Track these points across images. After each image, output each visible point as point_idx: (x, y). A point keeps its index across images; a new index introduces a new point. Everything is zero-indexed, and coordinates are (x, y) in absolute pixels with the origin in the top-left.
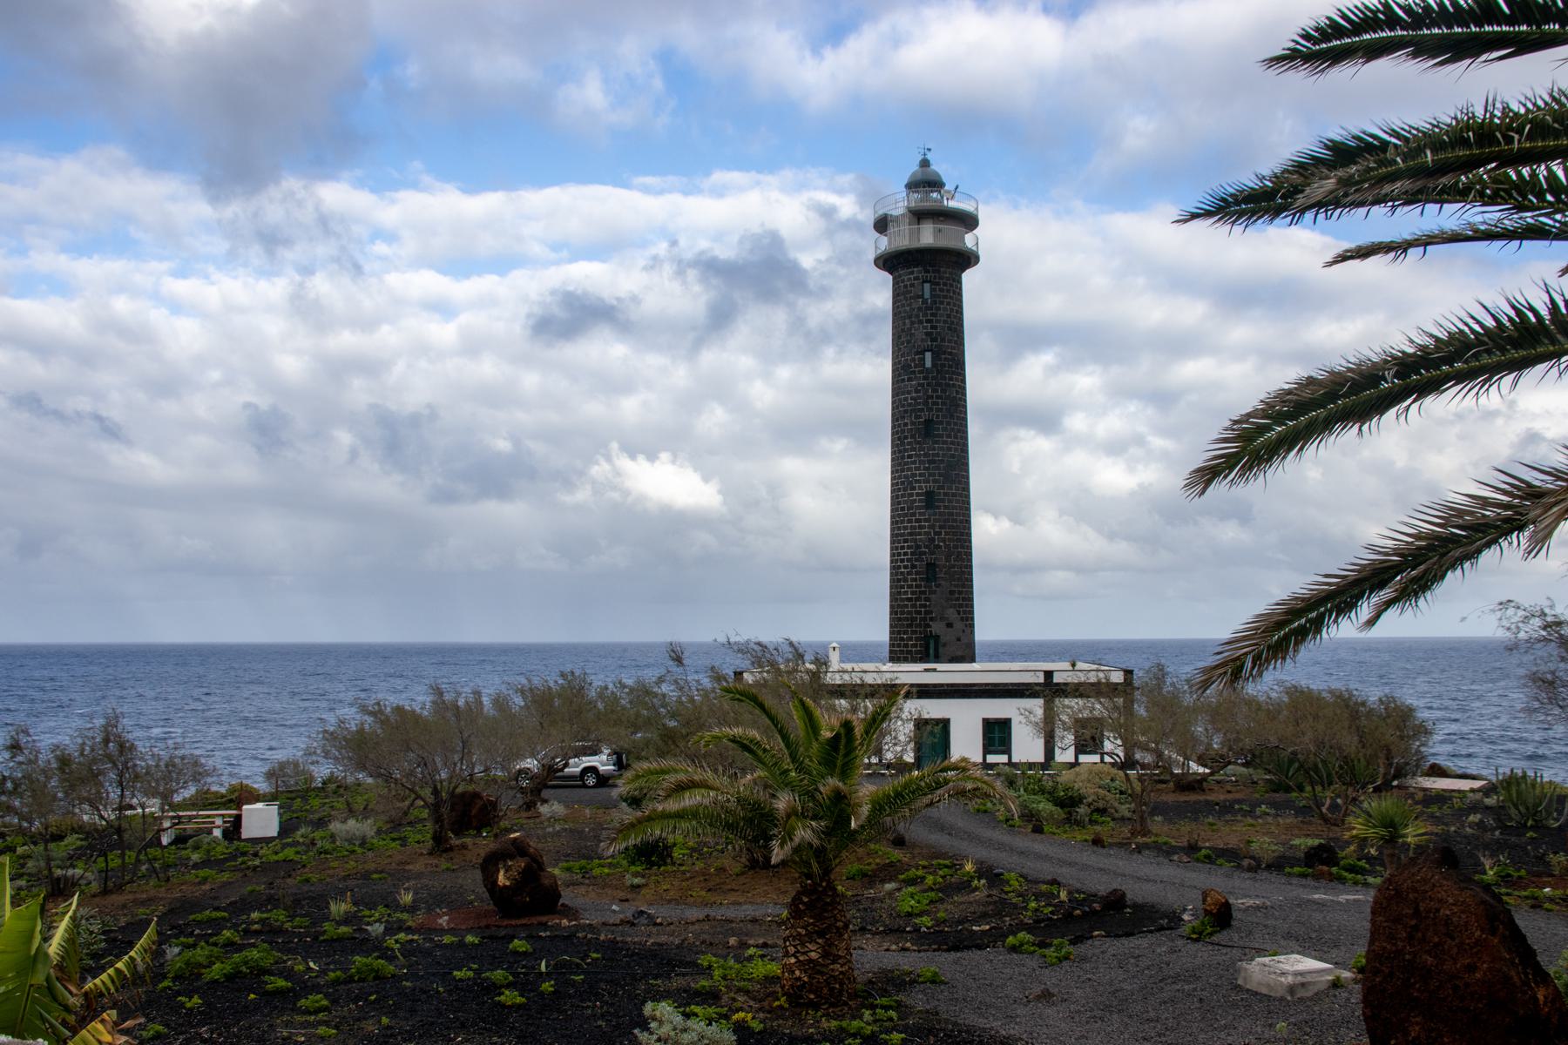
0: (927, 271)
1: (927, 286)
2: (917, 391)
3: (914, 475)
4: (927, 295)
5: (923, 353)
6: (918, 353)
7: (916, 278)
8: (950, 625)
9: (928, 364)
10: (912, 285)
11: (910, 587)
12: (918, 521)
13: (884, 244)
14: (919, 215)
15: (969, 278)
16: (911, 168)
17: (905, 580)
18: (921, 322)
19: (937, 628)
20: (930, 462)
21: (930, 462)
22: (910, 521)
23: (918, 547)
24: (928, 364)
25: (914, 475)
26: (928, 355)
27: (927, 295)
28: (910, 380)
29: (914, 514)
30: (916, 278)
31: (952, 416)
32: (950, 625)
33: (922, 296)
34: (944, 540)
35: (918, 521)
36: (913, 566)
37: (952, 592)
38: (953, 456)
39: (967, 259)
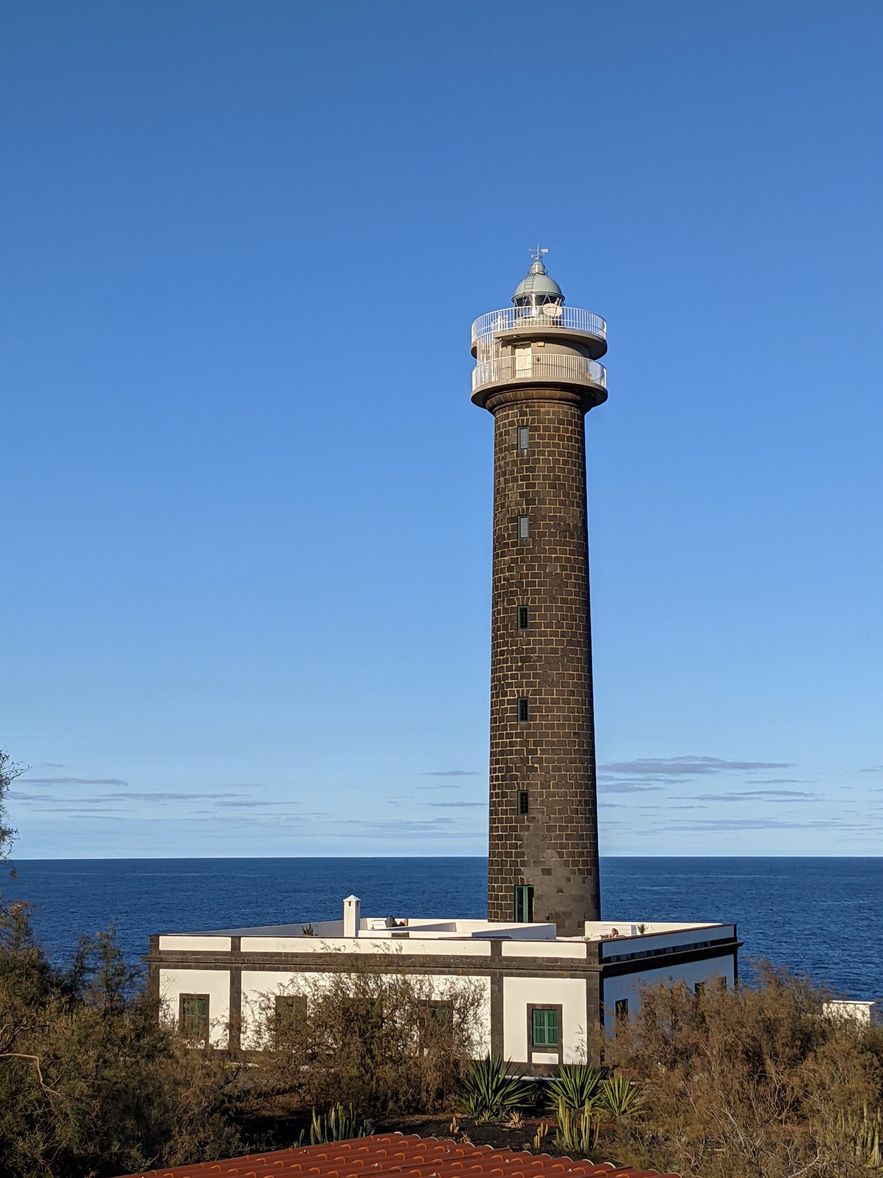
2: (510, 569)
3: (506, 677)
4: (524, 444)
6: (512, 520)
8: (547, 872)
9: (524, 533)
12: (509, 736)
18: (515, 480)
19: (530, 875)
20: (523, 660)
21: (523, 660)
23: (509, 769)
24: (524, 533)
26: (524, 522)
27: (524, 444)
30: (511, 424)
32: (547, 872)
33: (516, 447)
34: (540, 760)
35: (509, 736)
36: (504, 795)
37: (550, 828)
38: (554, 651)
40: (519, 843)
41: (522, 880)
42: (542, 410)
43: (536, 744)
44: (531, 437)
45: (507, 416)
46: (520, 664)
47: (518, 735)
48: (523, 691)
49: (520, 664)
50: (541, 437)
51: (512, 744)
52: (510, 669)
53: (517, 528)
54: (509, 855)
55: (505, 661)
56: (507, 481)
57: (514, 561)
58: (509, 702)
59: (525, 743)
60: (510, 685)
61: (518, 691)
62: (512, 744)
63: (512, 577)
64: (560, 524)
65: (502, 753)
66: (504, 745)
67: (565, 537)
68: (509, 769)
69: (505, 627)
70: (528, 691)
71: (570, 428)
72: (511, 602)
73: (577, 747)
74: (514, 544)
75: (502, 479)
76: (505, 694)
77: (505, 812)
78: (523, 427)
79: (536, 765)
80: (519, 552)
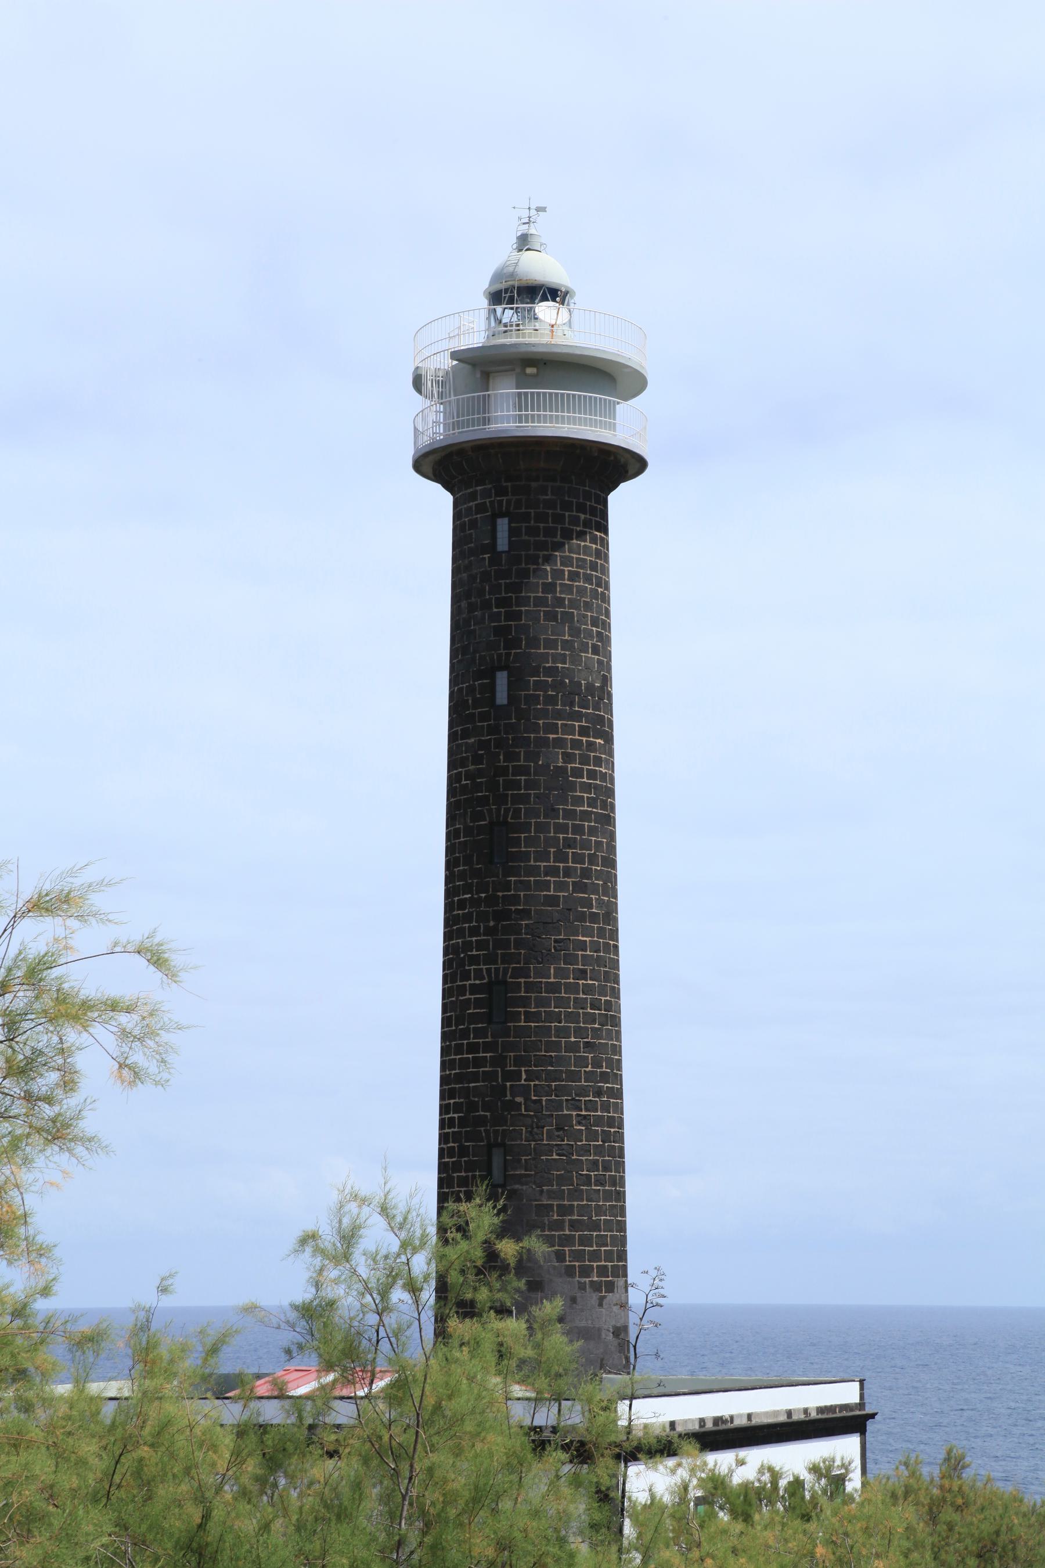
0: (501, 492)
1: (503, 525)
2: (477, 760)
3: (467, 946)
4: (502, 543)
5: (490, 673)
6: (479, 675)
9: (502, 697)
10: (473, 524)
12: (473, 1048)
16: (492, 257)
18: (486, 605)
23: (472, 1107)
25: (467, 946)
27: (502, 543)
29: (465, 1034)
31: (553, 812)
35: (473, 1048)
42: (534, 484)
43: (519, 1061)
44: (512, 532)
45: (473, 496)
46: (492, 923)
47: (487, 1047)
49: (492, 923)
50: (533, 531)
51: (478, 1062)
52: (474, 931)
53: (492, 688)
55: (468, 918)
56: (472, 608)
57: (483, 745)
58: (474, 989)
59: (499, 1061)
60: (474, 960)
61: (489, 970)
62: (478, 1062)
63: (480, 773)
64: (562, 683)
65: (459, 1078)
66: (464, 1063)
67: (572, 704)
68: (472, 1107)
69: (468, 860)
70: (506, 970)
71: (582, 516)
72: (477, 816)
73: (590, 1069)
74: (484, 717)
75: (464, 604)
76: (466, 976)
78: (502, 515)
79: (519, 1099)
80: (493, 730)
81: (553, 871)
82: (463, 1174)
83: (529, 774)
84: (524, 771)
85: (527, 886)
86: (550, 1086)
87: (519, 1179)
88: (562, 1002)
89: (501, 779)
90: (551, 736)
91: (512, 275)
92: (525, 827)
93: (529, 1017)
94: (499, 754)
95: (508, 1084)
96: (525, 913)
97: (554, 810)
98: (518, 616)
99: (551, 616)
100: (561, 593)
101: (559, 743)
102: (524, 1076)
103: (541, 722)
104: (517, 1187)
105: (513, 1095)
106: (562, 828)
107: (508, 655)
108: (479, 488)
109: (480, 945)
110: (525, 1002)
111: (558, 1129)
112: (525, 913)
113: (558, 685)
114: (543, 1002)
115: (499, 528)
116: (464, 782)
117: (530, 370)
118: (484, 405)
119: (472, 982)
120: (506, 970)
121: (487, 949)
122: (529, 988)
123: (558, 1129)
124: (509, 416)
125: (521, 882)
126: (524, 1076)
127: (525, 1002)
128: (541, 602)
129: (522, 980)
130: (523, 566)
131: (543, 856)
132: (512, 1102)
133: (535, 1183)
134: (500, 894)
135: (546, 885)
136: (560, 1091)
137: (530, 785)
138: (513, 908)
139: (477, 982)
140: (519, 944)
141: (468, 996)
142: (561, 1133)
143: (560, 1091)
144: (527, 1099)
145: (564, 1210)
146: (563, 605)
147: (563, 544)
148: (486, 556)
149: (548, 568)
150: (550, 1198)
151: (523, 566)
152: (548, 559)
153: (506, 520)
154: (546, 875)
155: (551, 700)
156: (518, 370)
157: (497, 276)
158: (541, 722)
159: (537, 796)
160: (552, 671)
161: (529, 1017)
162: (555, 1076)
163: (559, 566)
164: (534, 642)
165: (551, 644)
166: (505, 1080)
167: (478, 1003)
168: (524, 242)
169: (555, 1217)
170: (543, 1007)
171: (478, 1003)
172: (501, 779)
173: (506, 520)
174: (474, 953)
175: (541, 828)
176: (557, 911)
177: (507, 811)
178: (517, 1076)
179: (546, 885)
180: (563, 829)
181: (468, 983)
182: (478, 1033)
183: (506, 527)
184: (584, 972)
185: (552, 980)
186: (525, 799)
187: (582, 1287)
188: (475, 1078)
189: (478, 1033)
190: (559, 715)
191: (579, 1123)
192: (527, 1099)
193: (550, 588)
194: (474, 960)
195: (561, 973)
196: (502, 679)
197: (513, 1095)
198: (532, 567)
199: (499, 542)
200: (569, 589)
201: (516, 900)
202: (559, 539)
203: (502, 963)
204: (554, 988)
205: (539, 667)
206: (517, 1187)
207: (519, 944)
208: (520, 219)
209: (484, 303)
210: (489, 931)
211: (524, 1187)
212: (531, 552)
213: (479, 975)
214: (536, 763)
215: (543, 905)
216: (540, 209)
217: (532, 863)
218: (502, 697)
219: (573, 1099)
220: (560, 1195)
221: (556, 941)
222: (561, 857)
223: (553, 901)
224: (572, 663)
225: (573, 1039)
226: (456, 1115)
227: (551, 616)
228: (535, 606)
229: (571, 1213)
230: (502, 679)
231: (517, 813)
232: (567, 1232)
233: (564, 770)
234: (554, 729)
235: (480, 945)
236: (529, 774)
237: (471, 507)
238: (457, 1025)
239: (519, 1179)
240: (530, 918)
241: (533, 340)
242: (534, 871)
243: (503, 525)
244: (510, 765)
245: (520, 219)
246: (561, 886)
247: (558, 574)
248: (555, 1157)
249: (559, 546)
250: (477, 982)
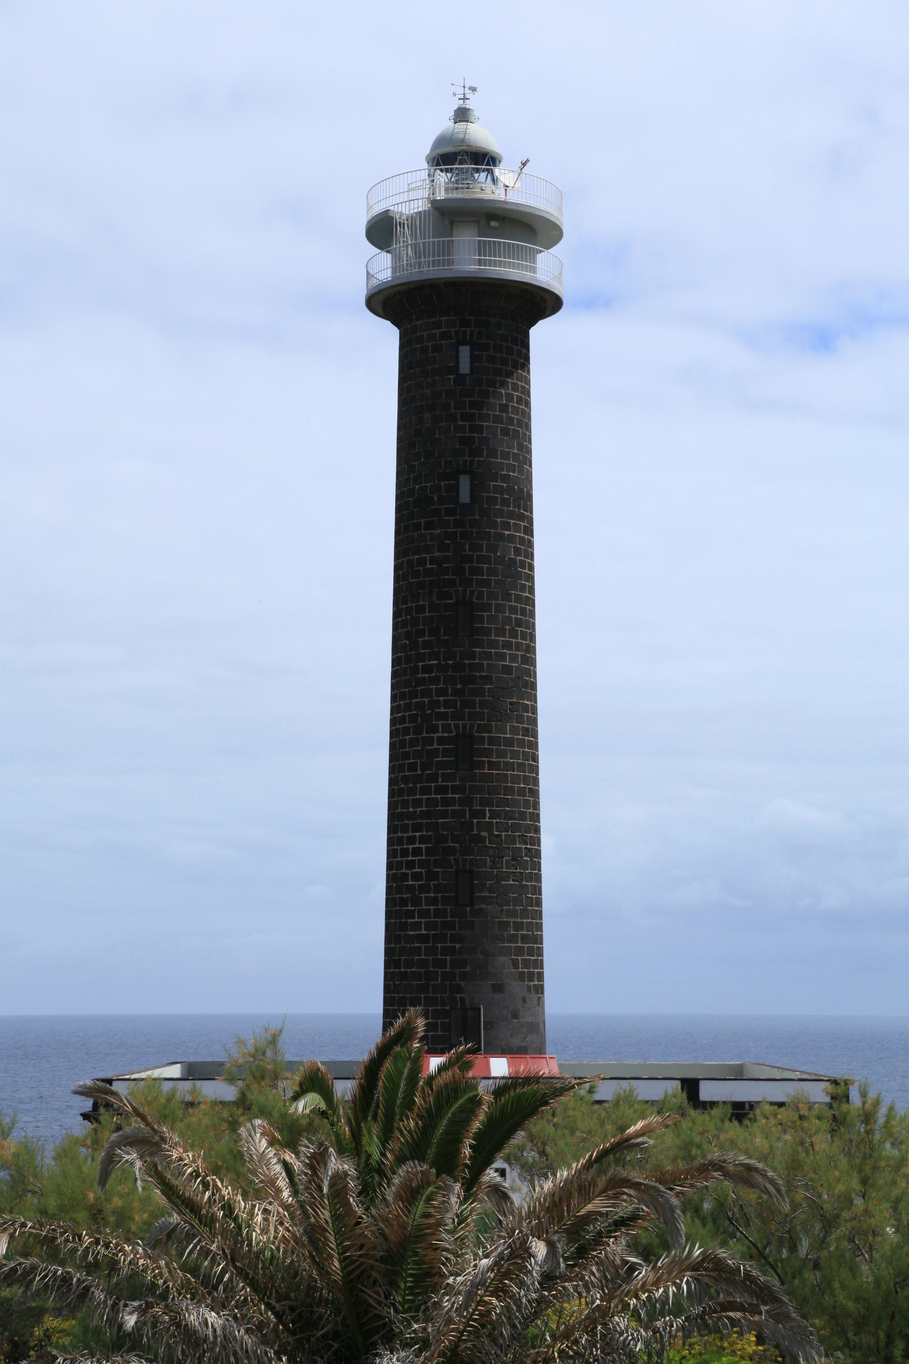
1: (465, 352)
3: (434, 704)
4: (465, 367)
7: (445, 336)
9: (465, 497)
11: (424, 914)
12: (440, 790)
13: (383, 267)
14: (449, 216)
15: (542, 336)
17: (416, 902)
22: (426, 791)
27: (465, 367)
28: (429, 526)
29: (433, 778)
30: (445, 336)
31: (507, 596)
35: (440, 790)
36: (431, 876)
39: (543, 303)
40: (458, 946)
41: (462, 999)
43: (485, 802)
44: (473, 359)
45: (438, 325)
46: (459, 686)
47: (455, 790)
48: (464, 726)
49: (459, 686)
51: (445, 802)
52: (440, 692)
53: (456, 488)
54: (443, 964)
55: (436, 681)
58: (441, 741)
60: (443, 716)
61: (457, 726)
62: (445, 802)
67: (519, 507)
75: (427, 415)
76: (435, 729)
77: (434, 901)
79: (484, 834)
81: (508, 645)
82: (432, 895)
83: (490, 563)
84: (482, 560)
85: (488, 656)
86: (507, 824)
87: (484, 900)
88: (515, 755)
89: (467, 566)
90: (507, 533)
91: (463, 141)
92: (488, 607)
93: (492, 765)
94: (465, 544)
95: (475, 821)
96: (487, 679)
97: (508, 594)
98: (480, 429)
99: (506, 432)
100: (512, 413)
101: (511, 538)
102: (488, 815)
103: (499, 520)
104: (483, 906)
105: (479, 830)
106: (513, 610)
107: (472, 462)
108: (443, 318)
109: (447, 704)
110: (488, 753)
111: (514, 859)
112: (487, 679)
113: (510, 490)
114: (501, 754)
115: (461, 354)
116: (428, 566)
117: (493, 224)
118: (447, 249)
119: (440, 734)
120: (472, 726)
121: (456, 707)
122: (492, 740)
123: (514, 859)
124: (469, 259)
125: (485, 653)
126: (488, 815)
127: (488, 753)
128: (497, 419)
129: (486, 735)
130: (484, 387)
131: (501, 632)
132: (478, 835)
133: (497, 903)
134: (467, 662)
135: (502, 657)
136: (514, 828)
137: (492, 572)
138: (478, 674)
139: (445, 735)
140: (483, 704)
141: (435, 746)
142: (514, 862)
143: (514, 828)
144: (491, 834)
145: (518, 926)
146: (512, 424)
147: (513, 373)
148: (452, 377)
149: (503, 392)
150: (508, 916)
151: (484, 387)
152: (503, 384)
153: (467, 348)
154: (503, 648)
155: (506, 503)
156: (483, 222)
157: (441, 141)
158: (499, 520)
159: (497, 582)
160: (506, 478)
161: (492, 765)
162: (509, 816)
163: (510, 391)
164: (493, 453)
165: (506, 455)
166: (472, 817)
167: (446, 753)
168: (462, 115)
169: (512, 932)
170: (502, 757)
171: (446, 753)
172: (467, 566)
173: (467, 348)
174: (442, 710)
175: (500, 609)
176: (512, 679)
177: (472, 592)
178: (482, 814)
179: (502, 657)
180: (513, 610)
181: (435, 735)
182: (445, 777)
183: (468, 354)
184: (527, 729)
185: (508, 736)
186: (486, 583)
187: (529, 990)
188: (444, 814)
189: (445, 777)
190: (511, 515)
191: (526, 855)
192: (491, 834)
193: (504, 408)
194: (443, 716)
195: (514, 730)
196: (465, 482)
197: (479, 830)
198: (492, 389)
199: (461, 365)
200: (516, 410)
201: (480, 667)
202: (510, 368)
203: (469, 720)
204: (509, 742)
205: (497, 473)
206: (483, 906)
207: (483, 704)
208: (455, 94)
209: (426, 165)
210: (456, 692)
211: (489, 907)
212: (491, 377)
213: (446, 728)
214: (495, 554)
215: (502, 672)
216: (473, 89)
217: (493, 637)
218: (465, 497)
219: (523, 835)
220: (513, 914)
221: (511, 703)
222: (513, 634)
223: (507, 670)
224: (519, 473)
225: (522, 786)
226: (423, 846)
227: (506, 432)
228: (494, 422)
229: (522, 930)
230: (465, 482)
231: (481, 594)
232: (520, 945)
233: (514, 561)
234: (507, 526)
235: (447, 704)
236: (490, 563)
237: (435, 334)
238: (422, 770)
239: (484, 900)
240: (492, 683)
241: (492, 197)
242: (493, 644)
243: (465, 352)
244: (475, 554)
245: (455, 94)
246: (513, 658)
247: (510, 397)
248: (511, 882)
249: (509, 374)
250: (445, 735)
